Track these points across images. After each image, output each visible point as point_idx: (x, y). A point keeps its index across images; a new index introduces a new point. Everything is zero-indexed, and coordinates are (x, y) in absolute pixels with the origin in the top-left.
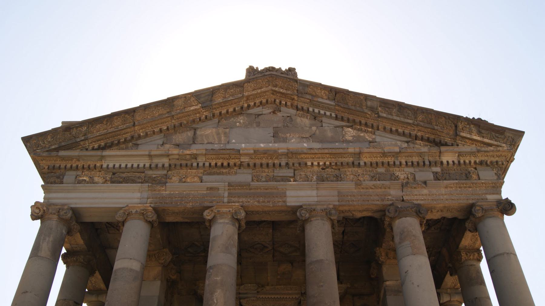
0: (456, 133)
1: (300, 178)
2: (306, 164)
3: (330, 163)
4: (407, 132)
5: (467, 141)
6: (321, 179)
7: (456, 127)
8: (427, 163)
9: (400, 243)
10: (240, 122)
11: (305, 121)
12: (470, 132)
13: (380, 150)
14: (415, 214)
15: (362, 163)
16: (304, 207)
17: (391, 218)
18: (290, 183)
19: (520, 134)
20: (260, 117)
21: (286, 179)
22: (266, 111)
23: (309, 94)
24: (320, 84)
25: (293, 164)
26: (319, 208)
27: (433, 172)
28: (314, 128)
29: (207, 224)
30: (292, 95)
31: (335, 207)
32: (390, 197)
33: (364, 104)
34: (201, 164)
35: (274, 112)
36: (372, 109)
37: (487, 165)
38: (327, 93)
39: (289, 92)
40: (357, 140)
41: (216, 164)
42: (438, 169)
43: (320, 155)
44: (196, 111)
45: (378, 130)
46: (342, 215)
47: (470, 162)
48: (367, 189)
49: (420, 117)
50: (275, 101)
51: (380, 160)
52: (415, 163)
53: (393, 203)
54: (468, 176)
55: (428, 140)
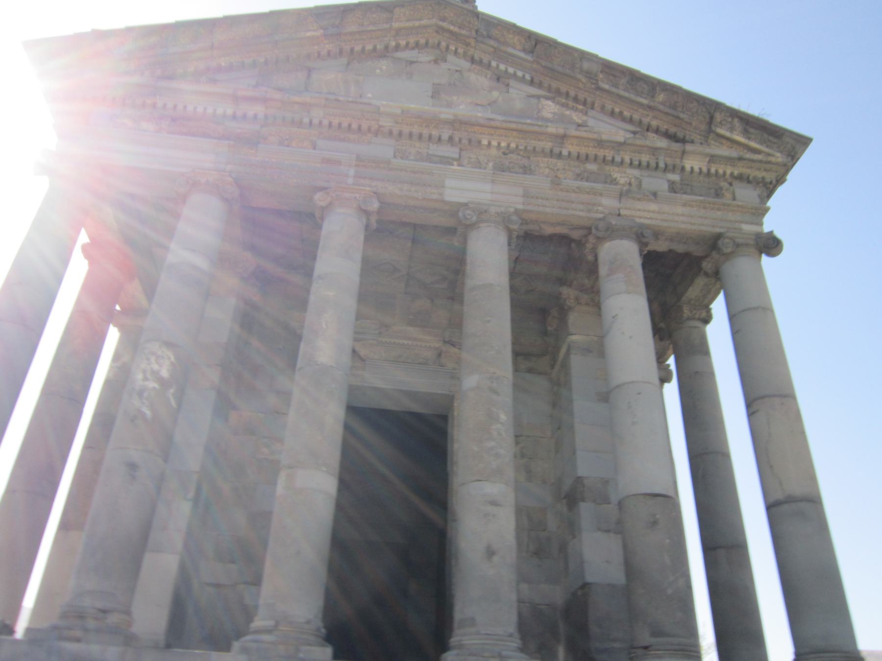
0: (710, 127)
1: (469, 163)
2: (479, 142)
3: (517, 147)
4: (636, 117)
5: (724, 141)
6: (501, 168)
7: (712, 118)
8: (662, 165)
9: (608, 275)
10: (381, 69)
11: (480, 80)
12: (732, 129)
13: (595, 136)
14: (634, 236)
15: (565, 152)
16: (471, 206)
17: (598, 238)
18: (452, 167)
19: (804, 142)
21: (446, 161)
22: (425, 57)
23: (496, 40)
24: (514, 26)
25: (460, 140)
26: (493, 210)
27: (669, 181)
28: (495, 94)
29: (317, 215)
30: (468, 37)
31: (517, 212)
32: (600, 208)
33: (578, 66)
34: (316, 121)
35: (436, 61)
36: (589, 75)
37: (749, 182)
38: (523, 41)
39: (464, 32)
41: (340, 125)
42: (675, 177)
43: (503, 131)
45: (592, 108)
46: (525, 228)
47: (725, 173)
48: (568, 191)
49: (661, 97)
50: (439, 44)
51: (592, 151)
53: (604, 217)
54: (718, 194)
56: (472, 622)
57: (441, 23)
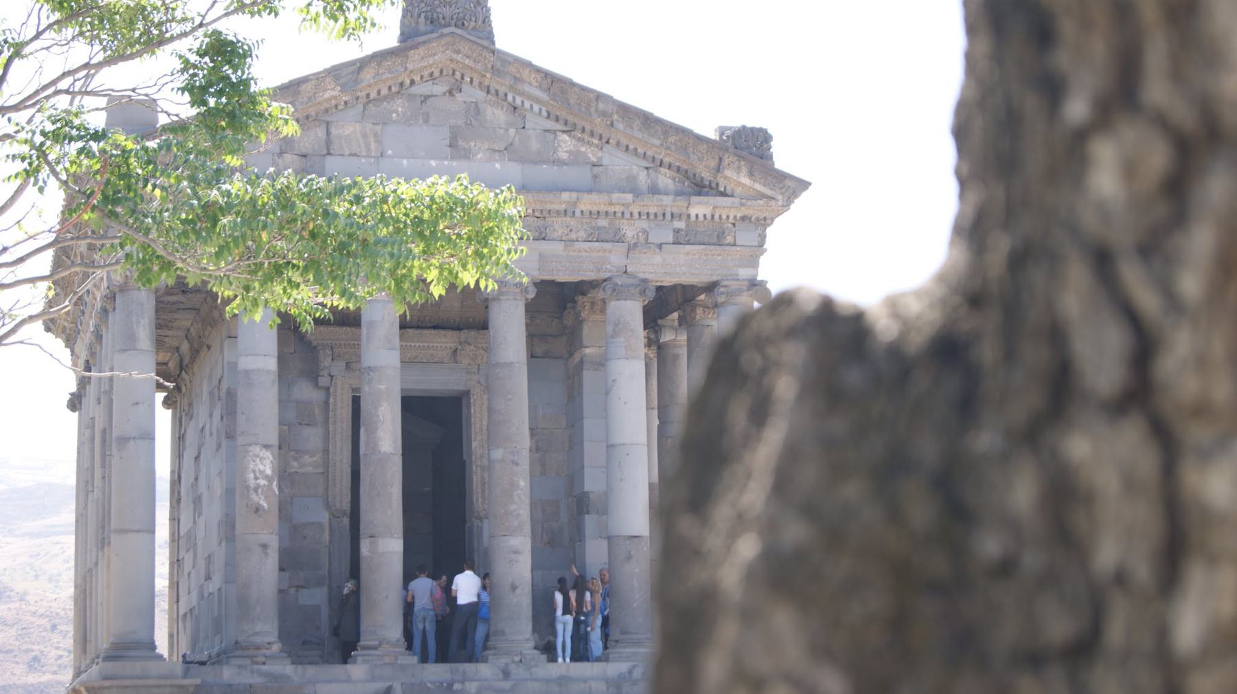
7: (721, 159)
8: (668, 216)
9: (612, 337)
10: (397, 112)
11: (497, 115)
12: (738, 170)
15: (578, 214)
20: (430, 101)
22: (439, 89)
24: (529, 65)
28: (512, 131)
33: (593, 104)
35: (450, 93)
39: (479, 67)
40: (576, 159)
44: (330, 99)
45: (607, 142)
47: (728, 217)
49: (672, 139)
50: (454, 72)
51: (603, 208)
52: (652, 217)
55: (678, 169)
56: (503, 633)
57: (455, 56)
